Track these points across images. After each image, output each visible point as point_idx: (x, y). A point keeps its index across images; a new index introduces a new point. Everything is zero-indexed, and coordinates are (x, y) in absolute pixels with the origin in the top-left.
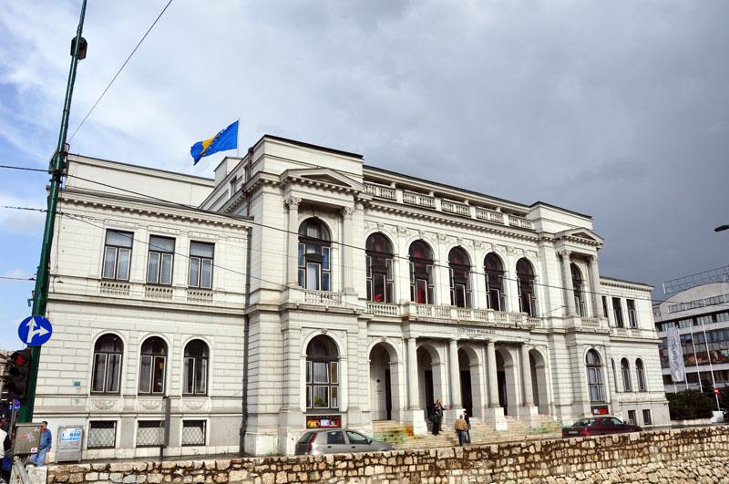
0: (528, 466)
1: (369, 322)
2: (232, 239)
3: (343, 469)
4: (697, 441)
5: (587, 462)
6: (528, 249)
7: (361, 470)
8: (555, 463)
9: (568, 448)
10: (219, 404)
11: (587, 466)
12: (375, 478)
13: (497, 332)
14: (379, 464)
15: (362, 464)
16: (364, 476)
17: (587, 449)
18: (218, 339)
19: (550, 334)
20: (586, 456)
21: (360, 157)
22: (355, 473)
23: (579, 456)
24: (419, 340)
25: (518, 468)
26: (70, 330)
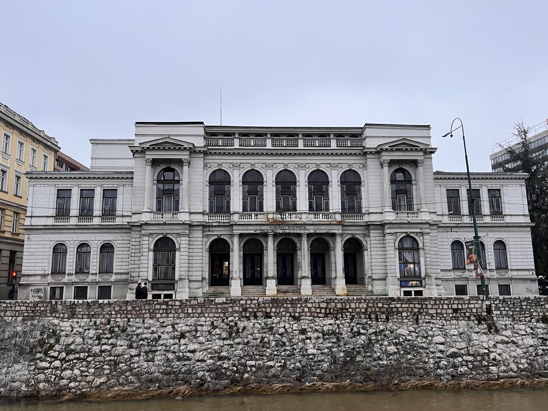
0: (121, 312)
1: (204, 226)
2: (127, 186)
3: (4, 307)
4: (289, 306)
5: (171, 313)
6: (355, 163)
7: (13, 308)
8: (144, 311)
9: (156, 304)
10: (119, 277)
11: (170, 315)
12: (20, 312)
13: (307, 227)
14: (23, 306)
15: (14, 305)
16: (15, 310)
17: (172, 306)
18: (118, 242)
19: (368, 226)
20: (171, 309)
21: (202, 123)
22: (10, 309)
23: (163, 309)
24: (241, 236)
25: (113, 313)
26: (39, 243)
